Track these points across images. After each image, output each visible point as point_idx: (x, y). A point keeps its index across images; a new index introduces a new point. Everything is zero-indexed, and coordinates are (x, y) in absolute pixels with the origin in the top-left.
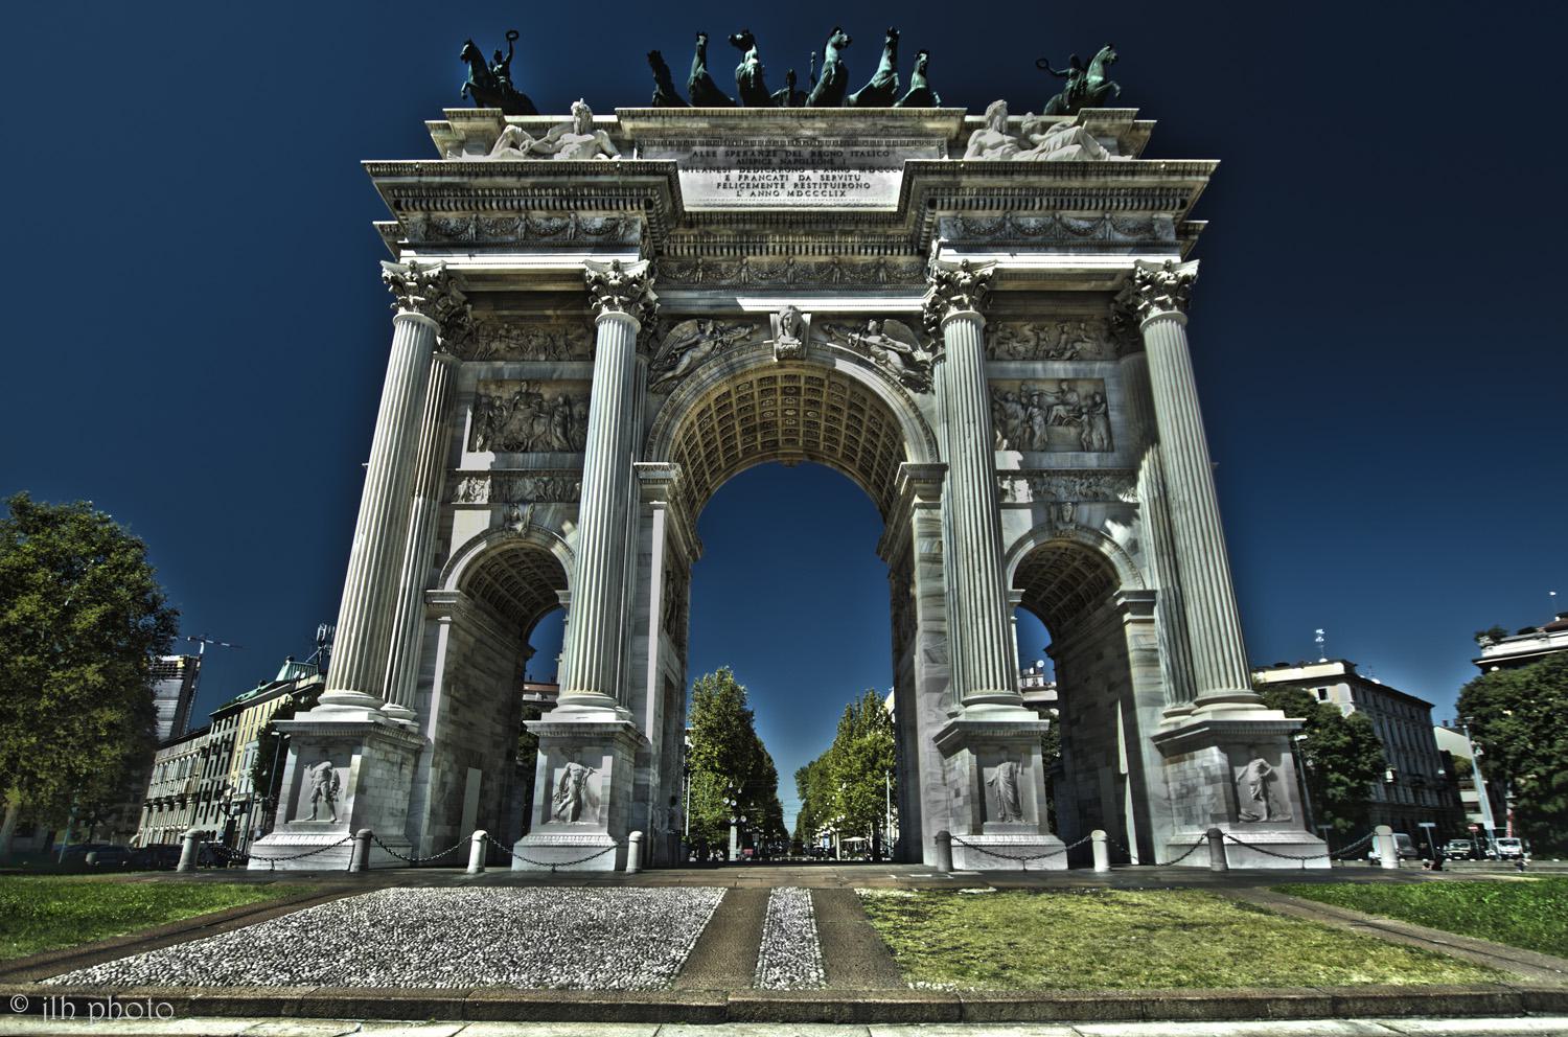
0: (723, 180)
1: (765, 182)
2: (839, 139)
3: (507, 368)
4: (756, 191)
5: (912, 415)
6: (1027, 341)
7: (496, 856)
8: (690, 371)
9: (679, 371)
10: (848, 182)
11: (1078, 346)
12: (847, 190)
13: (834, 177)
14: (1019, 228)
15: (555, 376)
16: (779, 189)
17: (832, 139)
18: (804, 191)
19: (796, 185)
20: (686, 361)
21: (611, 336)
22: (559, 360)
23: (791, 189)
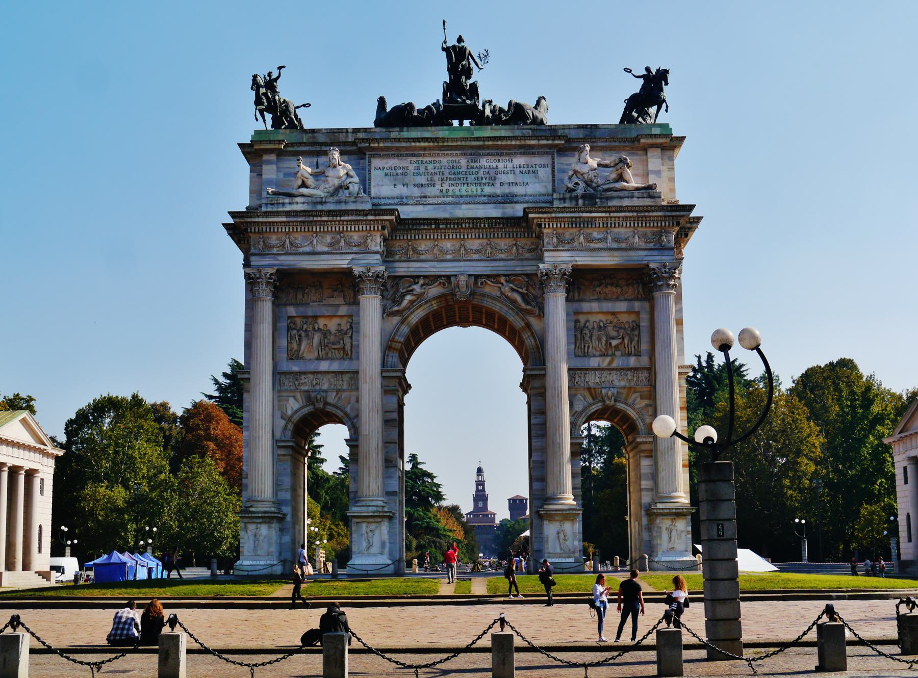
14: (589, 239)
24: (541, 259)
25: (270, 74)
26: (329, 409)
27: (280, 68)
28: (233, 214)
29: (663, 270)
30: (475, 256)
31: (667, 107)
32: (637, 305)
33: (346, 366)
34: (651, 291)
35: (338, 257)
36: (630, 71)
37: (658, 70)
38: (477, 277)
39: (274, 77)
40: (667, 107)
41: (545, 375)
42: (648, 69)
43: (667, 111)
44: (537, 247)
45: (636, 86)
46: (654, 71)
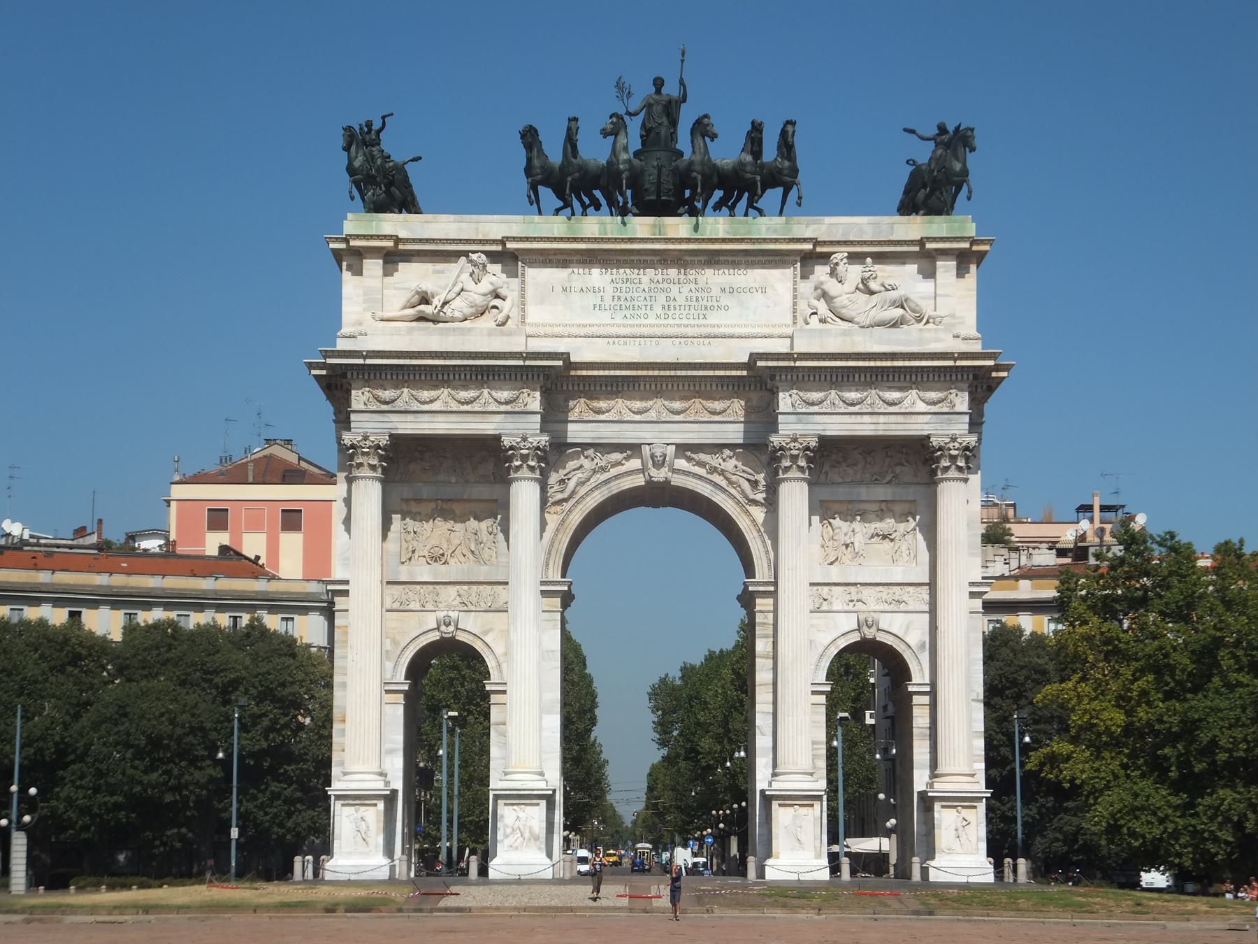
0: (598, 302)
1: (636, 303)
2: (702, 259)
3: (426, 491)
4: (628, 313)
5: (756, 534)
6: (855, 465)
7: (483, 871)
8: (573, 493)
9: (565, 495)
10: (709, 304)
11: (898, 469)
12: (708, 313)
13: (697, 299)
15: (465, 497)
16: (648, 312)
17: (696, 259)
18: (670, 313)
19: (663, 307)
20: (572, 484)
21: (524, 494)
22: (467, 482)
23: (659, 311)
24: (773, 427)
25: (369, 124)
26: (461, 637)
27: (383, 118)
28: (326, 354)
29: (951, 445)
30: (677, 418)
31: (970, 192)
32: (911, 492)
33: (482, 573)
34: (934, 472)
35: (478, 418)
36: (913, 132)
37: (957, 129)
38: (678, 446)
39: (376, 126)
40: (970, 192)
41: (776, 592)
42: (942, 129)
43: (969, 199)
44: (768, 405)
45: (924, 153)
46: (951, 129)
